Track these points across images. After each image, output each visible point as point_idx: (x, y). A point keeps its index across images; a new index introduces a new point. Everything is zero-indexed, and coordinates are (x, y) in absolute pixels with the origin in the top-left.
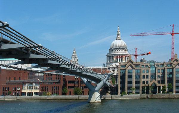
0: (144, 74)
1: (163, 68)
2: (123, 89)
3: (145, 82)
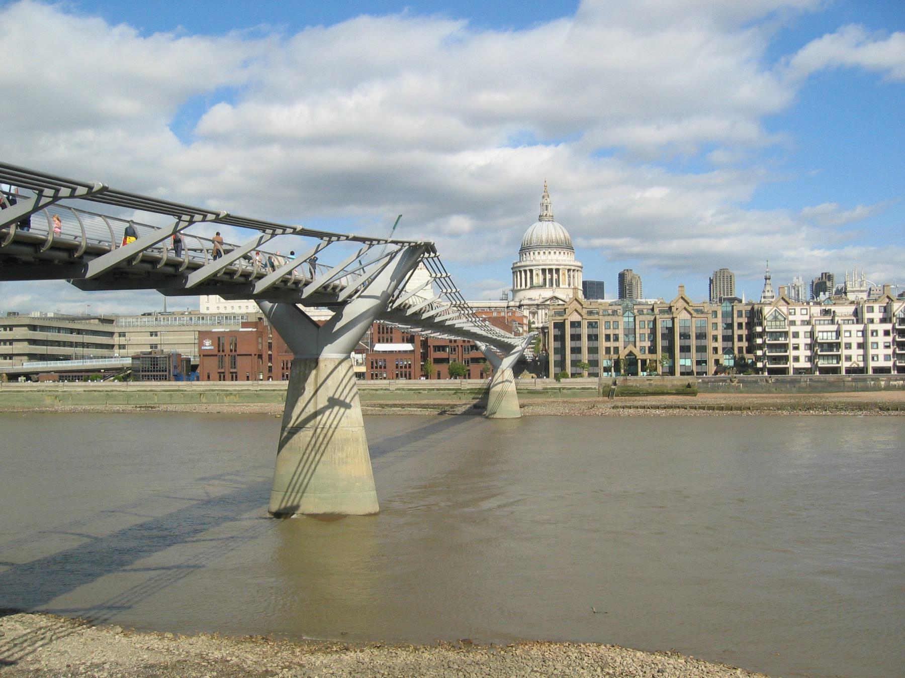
0: (608, 332)
1: (652, 318)
2: (561, 364)
3: (612, 349)
